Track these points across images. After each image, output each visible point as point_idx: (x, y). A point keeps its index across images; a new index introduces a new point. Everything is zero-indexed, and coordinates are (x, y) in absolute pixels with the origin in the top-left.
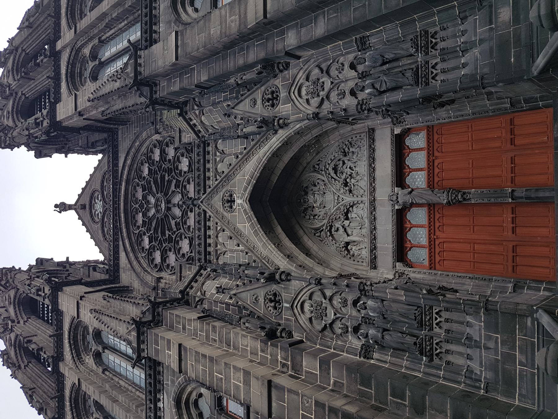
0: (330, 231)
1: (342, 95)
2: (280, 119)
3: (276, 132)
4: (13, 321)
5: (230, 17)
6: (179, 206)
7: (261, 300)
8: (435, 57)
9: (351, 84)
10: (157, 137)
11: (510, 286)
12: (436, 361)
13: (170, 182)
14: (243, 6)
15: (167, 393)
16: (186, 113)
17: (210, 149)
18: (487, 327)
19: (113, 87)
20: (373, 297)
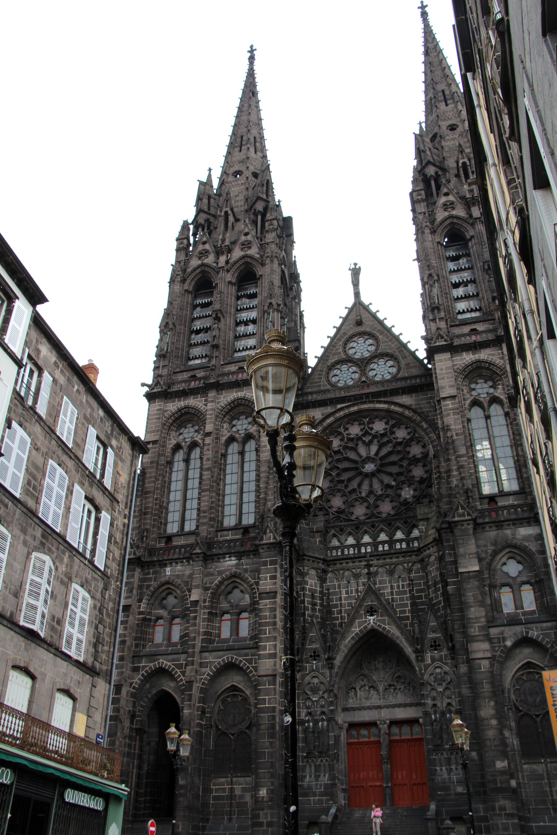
0: (361, 675)
1: (434, 699)
2: (421, 656)
3: (414, 652)
4: (227, 262)
5: (478, 627)
6: (371, 492)
7: (314, 646)
8: (447, 754)
9: (439, 704)
10: (432, 453)
11: (344, 787)
12: (305, 760)
13: (390, 474)
14: (481, 638)
15: (237, 565)
16: (437, 544)
17: (414, 557)
18: (325, 784)
19: (454, 476)
20: (328, 725)
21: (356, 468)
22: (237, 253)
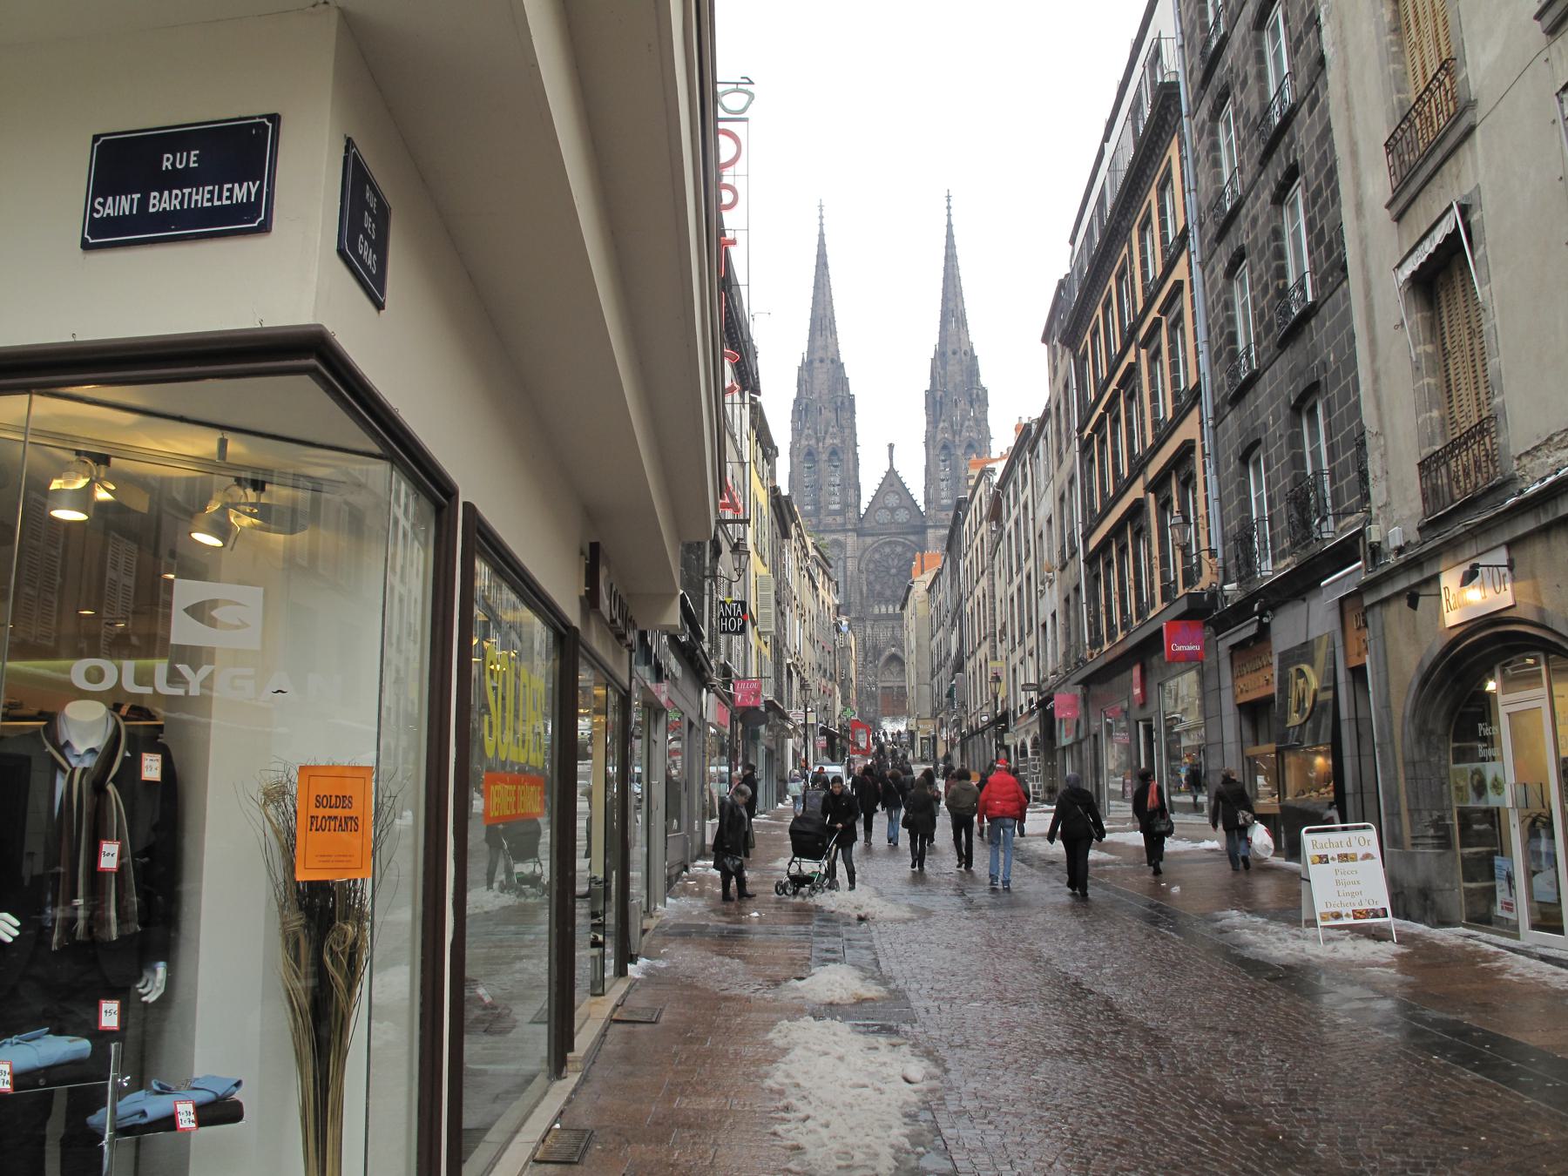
21: (888, 569)
22: (829, 441)
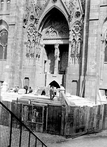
0: (51, 27)
